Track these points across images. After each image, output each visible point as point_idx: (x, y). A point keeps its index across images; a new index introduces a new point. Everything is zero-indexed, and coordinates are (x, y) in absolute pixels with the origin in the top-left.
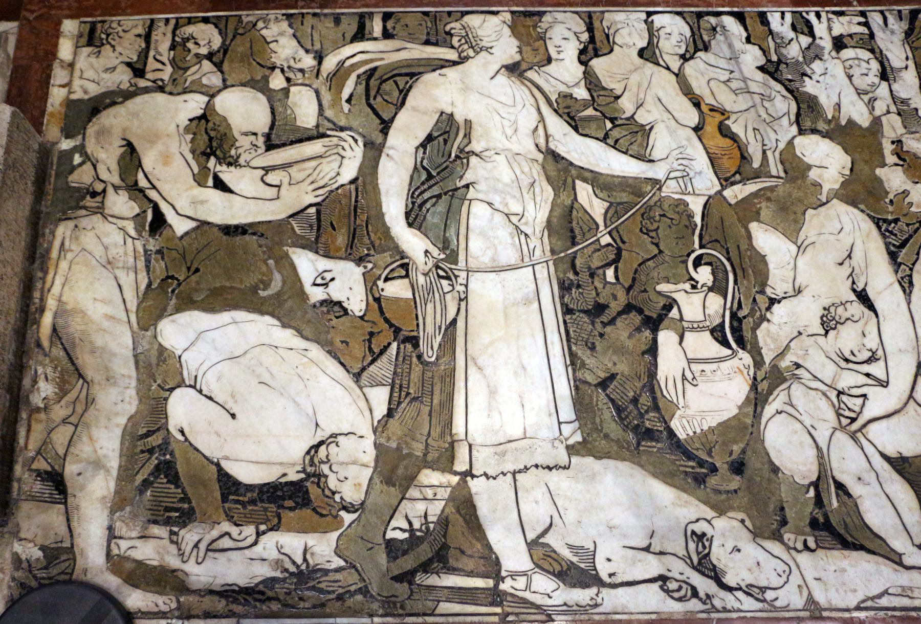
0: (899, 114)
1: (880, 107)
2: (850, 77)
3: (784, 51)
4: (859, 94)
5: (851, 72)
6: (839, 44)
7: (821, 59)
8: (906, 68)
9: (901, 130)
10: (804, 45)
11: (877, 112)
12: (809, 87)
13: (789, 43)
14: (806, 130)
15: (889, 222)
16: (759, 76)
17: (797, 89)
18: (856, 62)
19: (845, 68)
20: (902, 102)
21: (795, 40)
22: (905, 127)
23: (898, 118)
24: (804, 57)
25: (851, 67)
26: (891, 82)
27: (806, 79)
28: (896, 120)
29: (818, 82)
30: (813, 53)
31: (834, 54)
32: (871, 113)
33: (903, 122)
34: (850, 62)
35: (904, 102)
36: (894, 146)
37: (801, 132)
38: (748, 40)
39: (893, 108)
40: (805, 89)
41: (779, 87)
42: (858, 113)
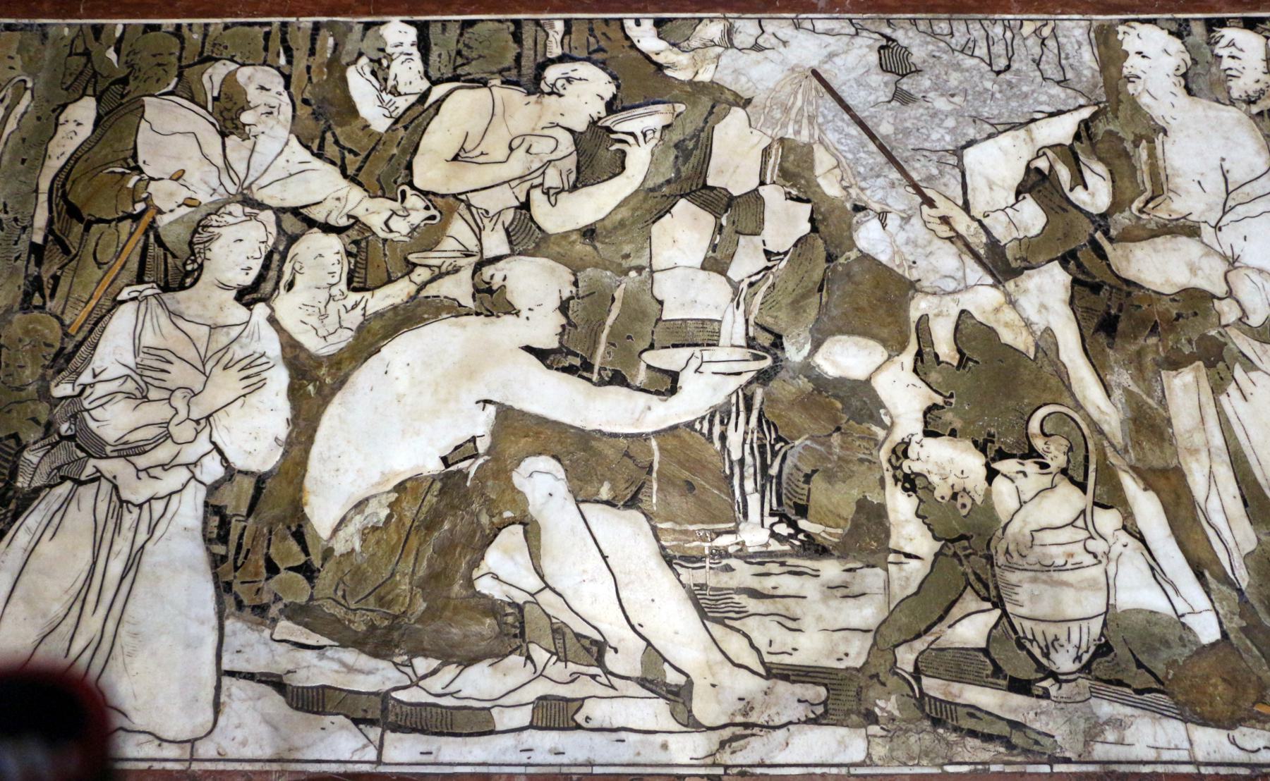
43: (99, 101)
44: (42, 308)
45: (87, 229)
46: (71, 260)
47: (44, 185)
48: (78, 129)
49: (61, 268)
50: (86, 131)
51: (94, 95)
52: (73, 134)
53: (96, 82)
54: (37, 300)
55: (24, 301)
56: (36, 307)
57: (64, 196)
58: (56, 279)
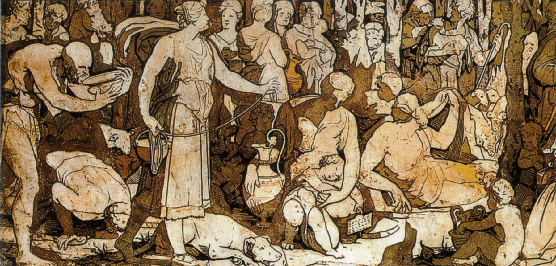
0: (385, 62)
1: (378, 58)
2: (367, 39)
3: (338, 23)
4: (369, 50)
5: (368, 37)
6: (367, 19)
7: (356, 29)
8: (397, 35)
9: (383, 71)
10: (349, 20)
11: (374, 61)
12: (346, 45)
13: (342, 19)
14: (337, 70)
15: (362, 118)
16: (322, 39)
17: (339, 46)
18: (373, 30)
19: (366, 34)
20: (389, 55)
21: (345, 17)
22: (386, 69)
23: (384, 64)
24: (347, 27)
25: (370, 33)
26: (387, 43)
27: (345, 40)
28: (383, 65)
29: (350, 42)
30: (353, 25)
31: (363, 26)
32: (372, 61)
33: (386, 66)
34: (369, 31)
35: (390, 55)
36: (377, 80)
37: (335, 71)
38: (322, 17)
39: (383, 59)
40: (342, 47)
41: (330, 45)
42: (365, 60)
43: (538, 33)
44: (533, 121)
45: (544, 89)
46: (540, 102)
47: (524, 72)
48: (533, 47)
49: (538, 105)
50: (536, 48)
51: (536, 31)
52: (531, 49)
53: (535, 25)
54: (531, 117)
55: (526, 118)
56: (531, 120)
57: (533, 75)
58: (536, 109)
